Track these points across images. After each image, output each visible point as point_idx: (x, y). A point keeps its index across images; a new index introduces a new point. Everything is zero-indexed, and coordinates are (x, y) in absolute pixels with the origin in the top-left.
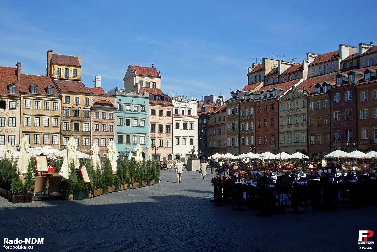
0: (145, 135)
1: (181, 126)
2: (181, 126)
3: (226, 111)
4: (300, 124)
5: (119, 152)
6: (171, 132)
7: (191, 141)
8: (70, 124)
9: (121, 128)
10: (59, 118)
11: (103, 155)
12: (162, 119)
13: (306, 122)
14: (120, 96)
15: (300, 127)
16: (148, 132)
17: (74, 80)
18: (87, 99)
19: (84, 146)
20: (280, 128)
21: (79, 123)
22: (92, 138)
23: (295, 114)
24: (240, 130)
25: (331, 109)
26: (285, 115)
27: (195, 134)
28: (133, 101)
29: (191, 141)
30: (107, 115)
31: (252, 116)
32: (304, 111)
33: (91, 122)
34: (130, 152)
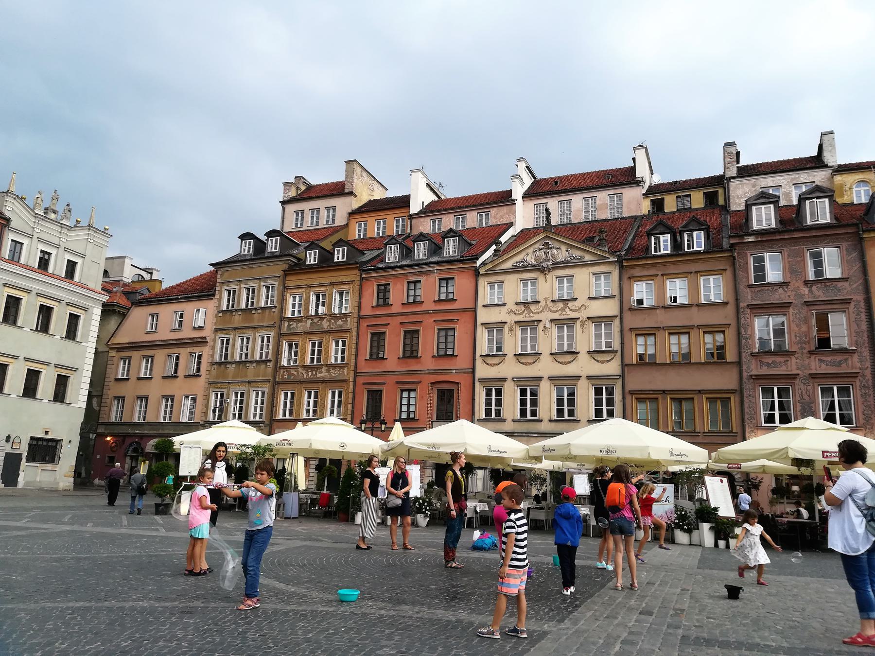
1: (28, 314)
2: (28, 314)
3: (214, 295)
4: (583, 357)
7: (62, 382)
13: (616, 346)
15: (584, 366)
20: (479, 361)
23: (556, 316)
24: (276, 363)
25: (743, 305)
26: (511, 319)
27: (82, 357)
29: (62, 382)
31: (344, 316)
32: (610, 308)
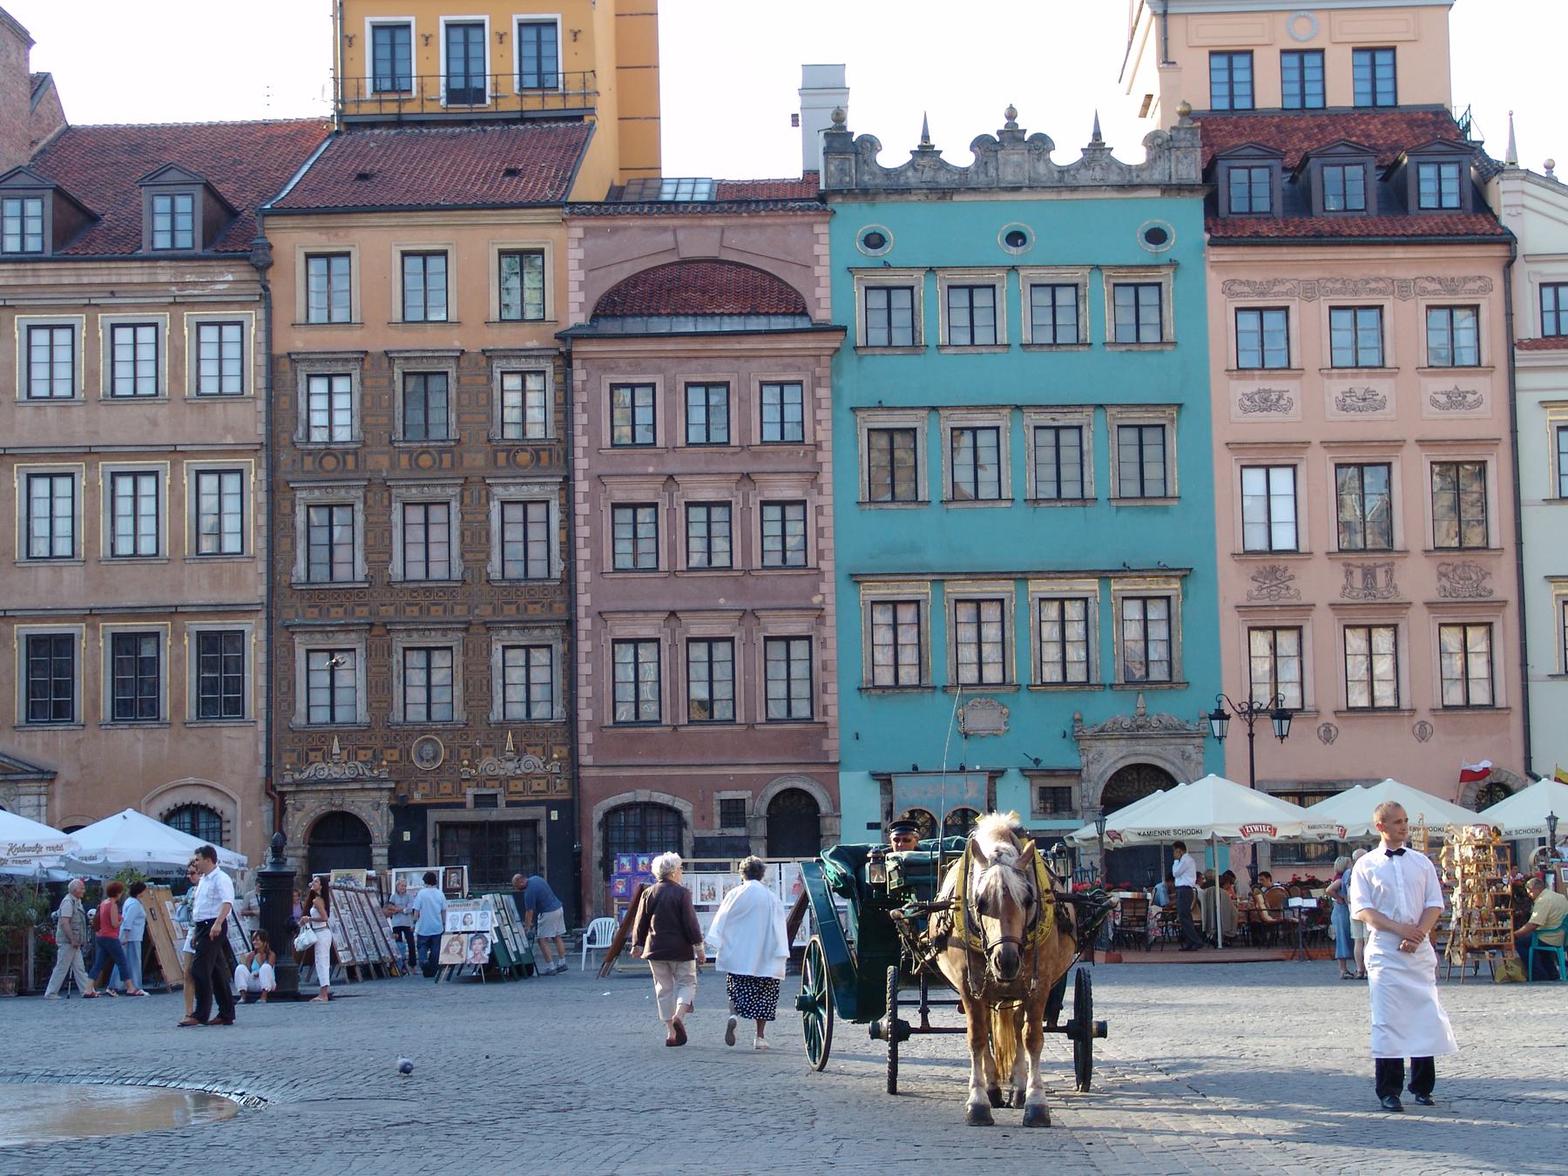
0: (1174, 586)
5: (885, 781)
6: (1499, 533)
8: (360, 518)
9: (894, 528)
10: (256, 478)
12: (1369, 401)
14: (866, 193)
16: (1210, 544)
17: (523, 118)
19: (505, 724)
21: (455, 505)
22: (584, 646)
28: (1015, 238)
30: (734, 401)
33: (567, 484)
34: (1013, 773)
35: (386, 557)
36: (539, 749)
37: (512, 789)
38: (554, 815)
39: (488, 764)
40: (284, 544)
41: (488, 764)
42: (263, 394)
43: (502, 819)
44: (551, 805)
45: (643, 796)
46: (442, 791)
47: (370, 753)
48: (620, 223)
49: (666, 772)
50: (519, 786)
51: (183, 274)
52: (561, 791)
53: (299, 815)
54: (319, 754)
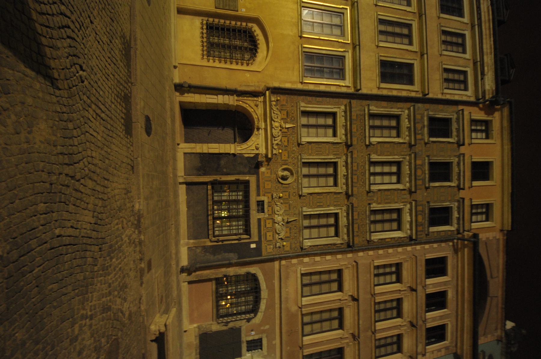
11: (253, 336)
18: (486, 210)
33: (411, 241)
35: (379, 153)
36: (288, 235)
37: (268, 221)
38: (253, 246)
39: (280, 209)
40: (384, 104)
41: (280, 209)
42: (444, 97)
43: (251, 217)
44: (259, 243)
45: (264, 294)
46: (266, 183)
47: (286, 144)
48: (501, 254)
49: (277, 306)
50: (269, 225)
51: (488, 67)
52: (268, 250)
53: (252, 104)
54: (285, 117)
